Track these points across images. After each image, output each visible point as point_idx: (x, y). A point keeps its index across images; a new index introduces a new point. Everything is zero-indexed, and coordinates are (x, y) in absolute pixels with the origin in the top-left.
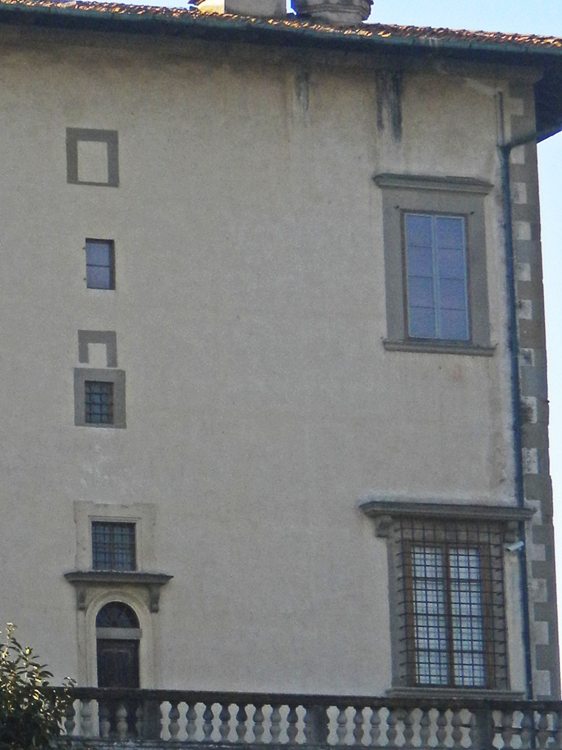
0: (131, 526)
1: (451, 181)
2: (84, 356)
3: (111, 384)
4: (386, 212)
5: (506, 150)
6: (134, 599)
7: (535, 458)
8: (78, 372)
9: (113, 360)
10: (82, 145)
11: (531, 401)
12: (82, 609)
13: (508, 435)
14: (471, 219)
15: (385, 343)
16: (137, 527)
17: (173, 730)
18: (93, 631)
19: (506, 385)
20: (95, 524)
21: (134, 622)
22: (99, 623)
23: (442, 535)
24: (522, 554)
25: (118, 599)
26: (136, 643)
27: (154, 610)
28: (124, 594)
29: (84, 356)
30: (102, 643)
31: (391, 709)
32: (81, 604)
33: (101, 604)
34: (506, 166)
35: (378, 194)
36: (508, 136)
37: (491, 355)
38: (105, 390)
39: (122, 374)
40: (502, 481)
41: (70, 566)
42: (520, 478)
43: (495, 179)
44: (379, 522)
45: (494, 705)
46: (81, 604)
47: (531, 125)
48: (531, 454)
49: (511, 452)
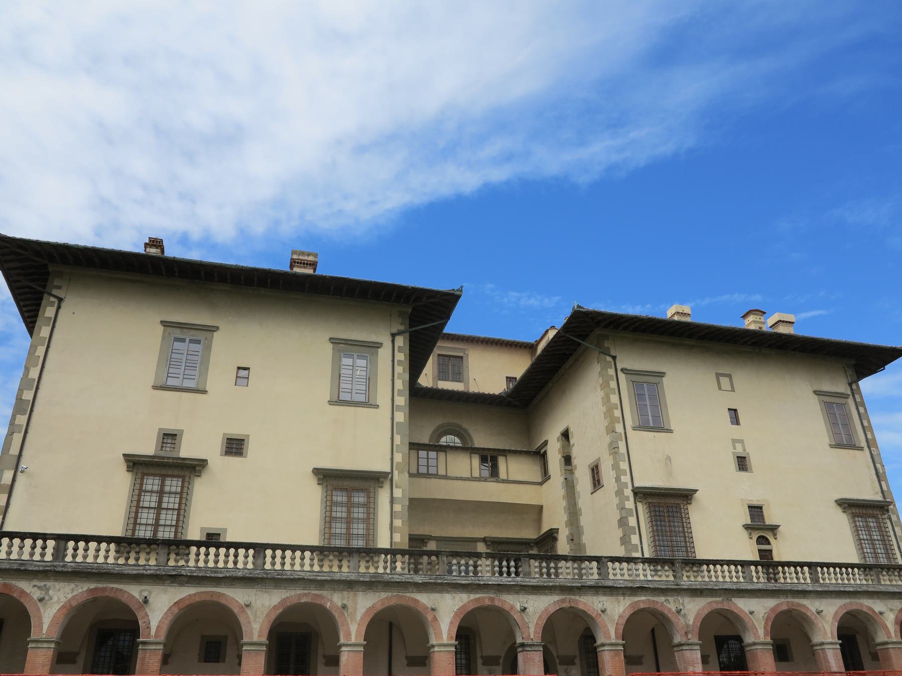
0: (761, 508)
1: (836, 393)
2: (734, 448)
3: (745, 458)
4: (820, 402)
5: (850, 385)
6: (768, 535)
8: (734, 453)
10: (720, 378)
11: (878, 466)
12: (751, 538)
13: (875, 477)
15: (830, 445)
16: (764, 508)
17: (824, 579)
18: (756, 547)
19: (870, 460)
20: (749, 507)
21: (769, 543)
26: (771, 551)
27: (776, 539)
28: (766, 533)
29: (734, 448)
30: (760, 551)
32: (751, 536)
33: (757, 536)
34: (852, 389)
35: (816, 397)
38: (742, 460)
39: (748, 454)
40: (877, 493)
42: (882, 491)
43: (849, 392)
44: (843, 507)
46: (751, 536)
47: (855, 378)
48: (883, 483)
49: (877, 483)
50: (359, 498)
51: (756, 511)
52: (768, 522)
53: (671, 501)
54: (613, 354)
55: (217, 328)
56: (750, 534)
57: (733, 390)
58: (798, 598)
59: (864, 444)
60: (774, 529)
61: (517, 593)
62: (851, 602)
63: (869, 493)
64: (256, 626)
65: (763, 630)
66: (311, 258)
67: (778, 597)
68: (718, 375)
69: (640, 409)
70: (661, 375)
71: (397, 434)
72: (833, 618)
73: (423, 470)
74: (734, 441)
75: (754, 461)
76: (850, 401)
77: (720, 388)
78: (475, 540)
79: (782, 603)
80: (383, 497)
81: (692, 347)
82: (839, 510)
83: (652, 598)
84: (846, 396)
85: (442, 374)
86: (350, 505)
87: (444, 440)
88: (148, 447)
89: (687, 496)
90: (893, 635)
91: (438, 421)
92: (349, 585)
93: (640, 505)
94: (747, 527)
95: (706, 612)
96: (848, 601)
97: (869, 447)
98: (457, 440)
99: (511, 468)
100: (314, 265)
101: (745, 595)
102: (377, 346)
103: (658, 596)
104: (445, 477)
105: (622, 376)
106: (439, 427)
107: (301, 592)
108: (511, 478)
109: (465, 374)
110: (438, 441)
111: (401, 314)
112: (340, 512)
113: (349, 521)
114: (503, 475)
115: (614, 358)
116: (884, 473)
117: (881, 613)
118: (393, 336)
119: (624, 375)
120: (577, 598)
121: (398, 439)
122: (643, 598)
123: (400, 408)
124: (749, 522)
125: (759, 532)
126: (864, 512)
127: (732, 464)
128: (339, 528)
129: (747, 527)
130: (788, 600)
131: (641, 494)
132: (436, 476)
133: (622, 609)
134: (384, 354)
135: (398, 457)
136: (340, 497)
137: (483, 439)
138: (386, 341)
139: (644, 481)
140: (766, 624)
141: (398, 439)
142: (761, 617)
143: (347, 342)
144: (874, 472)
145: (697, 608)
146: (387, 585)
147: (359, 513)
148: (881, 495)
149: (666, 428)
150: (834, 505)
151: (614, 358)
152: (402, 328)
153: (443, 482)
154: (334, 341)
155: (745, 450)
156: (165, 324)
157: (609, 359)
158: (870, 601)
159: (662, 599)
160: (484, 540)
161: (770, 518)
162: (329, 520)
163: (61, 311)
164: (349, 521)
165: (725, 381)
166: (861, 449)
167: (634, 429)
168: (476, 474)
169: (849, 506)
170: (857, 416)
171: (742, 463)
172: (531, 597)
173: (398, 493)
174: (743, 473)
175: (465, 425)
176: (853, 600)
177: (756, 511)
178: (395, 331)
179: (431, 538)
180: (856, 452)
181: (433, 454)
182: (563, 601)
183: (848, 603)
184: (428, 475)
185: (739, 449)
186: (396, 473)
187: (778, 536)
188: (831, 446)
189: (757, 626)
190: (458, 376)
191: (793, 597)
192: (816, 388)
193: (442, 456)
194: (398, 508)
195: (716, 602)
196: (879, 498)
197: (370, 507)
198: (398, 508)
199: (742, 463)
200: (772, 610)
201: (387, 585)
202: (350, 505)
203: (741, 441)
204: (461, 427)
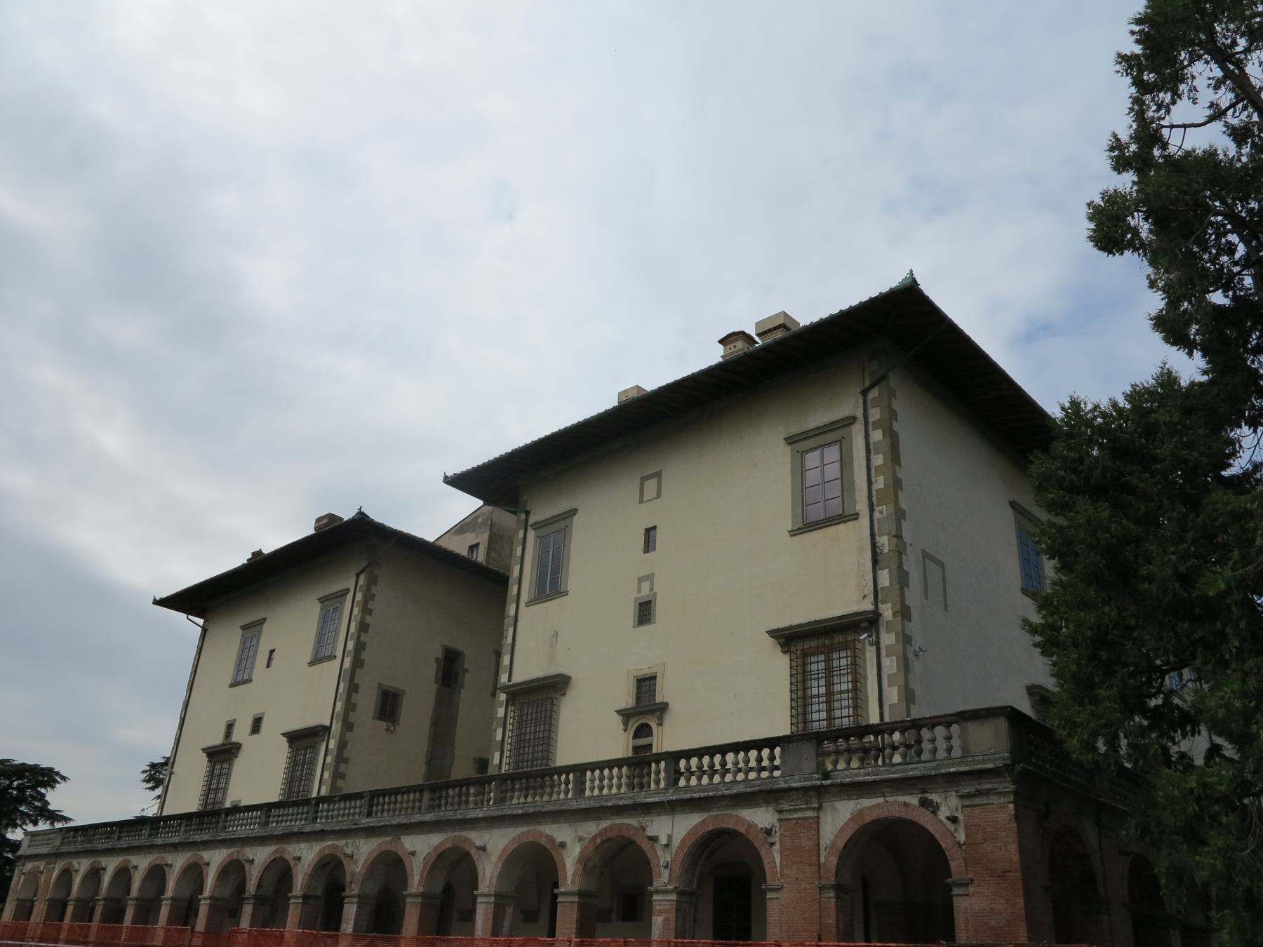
0: (655, 678)
2: (639, 591)
4: (793, 457)
7: (888, 576)
8: (636, 600)
9: (652, 590)
13: (869, 565)
14: (844, 442)
18: (631, 743)
22: (636, 736)
24: (877, 644)
25: (644, 721)
29: (639, 591)
31: (629, 766)
33: (636, 726)
34: (865, 402)
35: (788, 448)
36: (867, 384)
37: (857, 519)
39: (655, 594)
40: (865, 596)
41: (622, 706)
43: (859, 413)
51: (646, 684)
52: (659, 699)
54: (528, 508)
55: (265, 619)
56: (626, 724)
57: (659, 495)
58: (466, 829)
59: (862, 506)
60: (664, 707)
61: (252, 845)
62: (528, 831)
65: (418, 877)
67: (445, 831)
70: (575, 511)
71: (343, 681)
72: (499, 858)
74: (641, 580)
77: (641, 501)
79: (448, 838)
83: (335, 842)
84: (852, 420)
88: (217, 739)
90: (569, 881)
94: (626, 715)
95: (374, 855)
96: (525, 829)
97: (872, 510)
101: (413, 831)
103: (342, 839)
107: (157, 855)
117: (563, 845)
118: (358, 576)
119: (534, 532)
120: (285, 846)
122: (330, 843)
125: (637, 720)
126: (827, 642)
129: (626, 715)
130: (456, 834)
133: (313, 856)
140: (424, 867)
142: (422, 860)
144: (868, 555)
145: (368, 851)
148: (871, 598)
149: (562, 591)
151: (528, 513)
152: (364, 564)
155: (652, 590)
156: (244, 628)
158: (555, 826)
159: (342, 843)
161: (664, 693)
163: (206, 639)
166: (855, 516)
169: (788, 638)
170: (863, 453)
171: (645, 612)
172: (260, 848)
176: (531, 828)
177: (646, 684)
180: (842, 527)
182: (276, 851)
183: (523, 833)
186: (334, 722)
187: (669, 719)
189: (415, 872)
191: (461, 830)
192: (794, 430)
194: (329, 759)
195: (385, 842)
196: (868, 606)
198: (329, 759)
199: (645, 612)
200: (436, 848)
203: (650, 577)
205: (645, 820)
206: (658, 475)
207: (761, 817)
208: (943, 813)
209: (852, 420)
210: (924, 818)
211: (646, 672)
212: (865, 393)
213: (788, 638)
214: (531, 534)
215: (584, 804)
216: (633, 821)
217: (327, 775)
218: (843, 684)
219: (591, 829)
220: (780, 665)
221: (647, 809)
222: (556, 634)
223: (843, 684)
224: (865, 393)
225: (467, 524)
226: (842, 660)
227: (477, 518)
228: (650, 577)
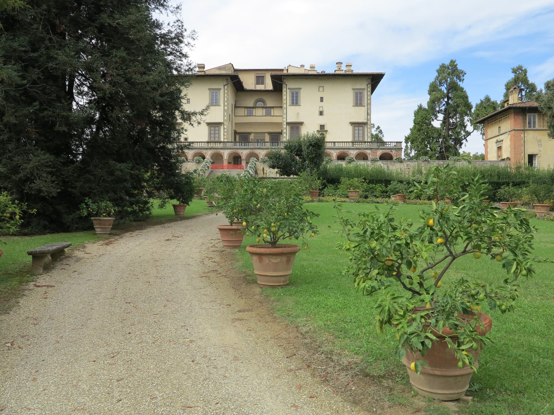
11: (369, 111)
23: (357, 125)
45: (354, 142)
50: (217, 129)
51: (322, 127)
53: (295, 125)
59: (366, 105)
60: (326, 131)
63: (362, 120)
64: (190, 157)
66: (202, 66)
68: (319, 87)
69: (293, 100)
70: (301, 88)
73: (249, 114)
74: (320, 107)
75: (325, 113)
76: (366, 91)
77: (319, 91)
78: (265, 133)
80: (222, 128)
81: (313, 78)
82: (350, 125)
84: (364, 89)
85: (258, 83)
86: (215, 130)
87: (260, 104)
89: (301, 123)
91: (256, 98)
92: (207, 149)
93: (287, 127)
98: (262, 103)
99: (276, 112)
100: (204, 68)
102: (220, 89)
104: (255, 116)
105: (288, 90)
106: (256, 100)
108: (275, 115)
109: (265, 81)
110: (256, 105)
111: (227, 80)
112: (212, 132)
113: (215, 134)
114: (272, 114)
115: (286, 85)
116: (370, 113)
118: (224, 86)
121: (225, 114)
123: (226, 106)
124: (319, 129)
127: (318, 113)
128: (213, 135)
131: (288, 124)
132: (253, 116)
134: (222, 91)
135: (225, 118)
136: (212, 129)
137: (269, 104)
138: (222, 87)
139: (289, 121)
141: (225, 114)
143: (212, 89)
146: (214, 149)
147: (217, 132)
150: (349, 123)
151: (286, 85)
152: (226, 83)
153: (254, 117)
154: (209, 89)
157: (285, 85)
160: (267, 132)
162: (210, 134)
164: (215, 134)
165: (321, 89)
166: (365, 106)
167: (289, 106)
168: (264, 114)
169: (352, 124)
171: (321, 113)
173: (225, 127)
174: (321, 116)
175: (264, 99)
178: (224, 84)
179: (252, 133)
181: (251, 109)
184: (250, 116)
185: (321, 109)
187: (327, 133)
188: (353, 106)
190: (263, 83)
193: (254, 109)
194: (225, 130)
196: (366, 121)
197: (219, 130)
199: (321, 113)
201: (214, 149)
202: (215, 130)
203: (322, 107)
204: (262, 99)
205: (349, 150)
206: (323, 87)
207: (368, 151)
208: (393, 153)
209: (364, 89)
210: (391, 153)
211: (322, 124)
212: (367, 85)
213: (352, 124)
214: (287, 90)
215: (334, 147)
216: (346, 150)
217: (225, 134)
218: (361, 132)
219: (338, 151)
220: (350, 128)
221: (349, 149)
222: (298, 113)
223: (361, 132)
224: (367, 85)
225: (222, 68)
226: (361, 128)
227: (226, 67)
228: (322, 107)
